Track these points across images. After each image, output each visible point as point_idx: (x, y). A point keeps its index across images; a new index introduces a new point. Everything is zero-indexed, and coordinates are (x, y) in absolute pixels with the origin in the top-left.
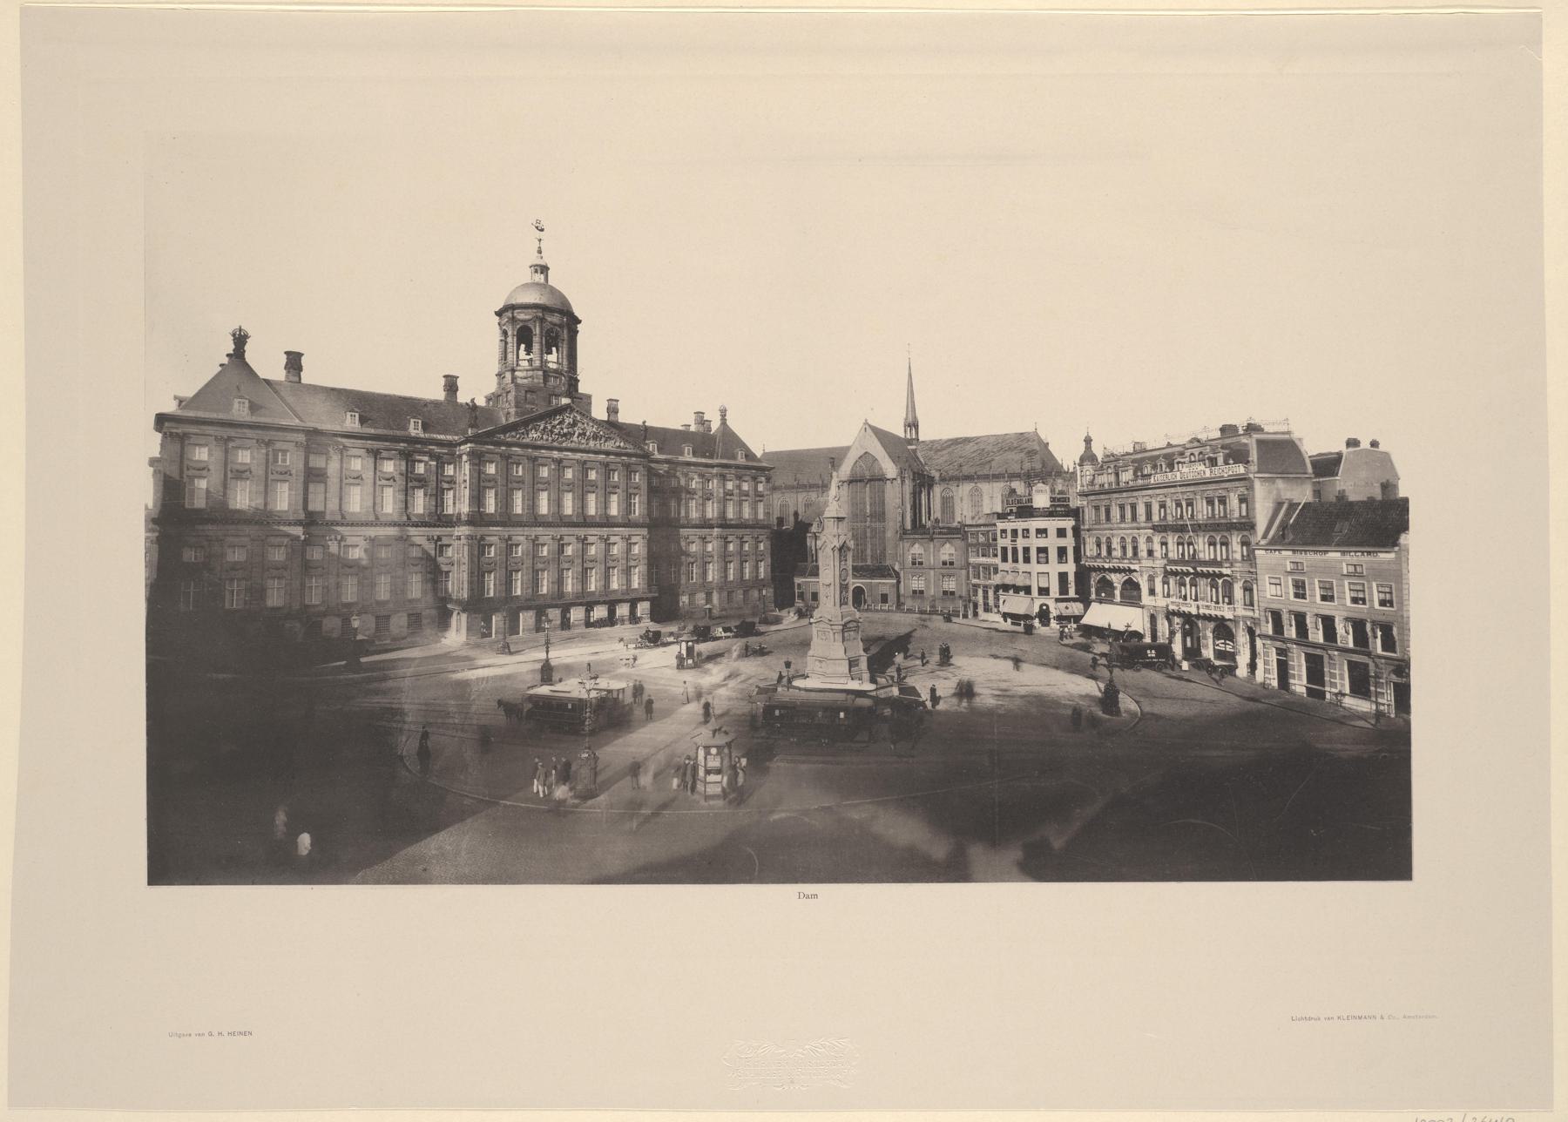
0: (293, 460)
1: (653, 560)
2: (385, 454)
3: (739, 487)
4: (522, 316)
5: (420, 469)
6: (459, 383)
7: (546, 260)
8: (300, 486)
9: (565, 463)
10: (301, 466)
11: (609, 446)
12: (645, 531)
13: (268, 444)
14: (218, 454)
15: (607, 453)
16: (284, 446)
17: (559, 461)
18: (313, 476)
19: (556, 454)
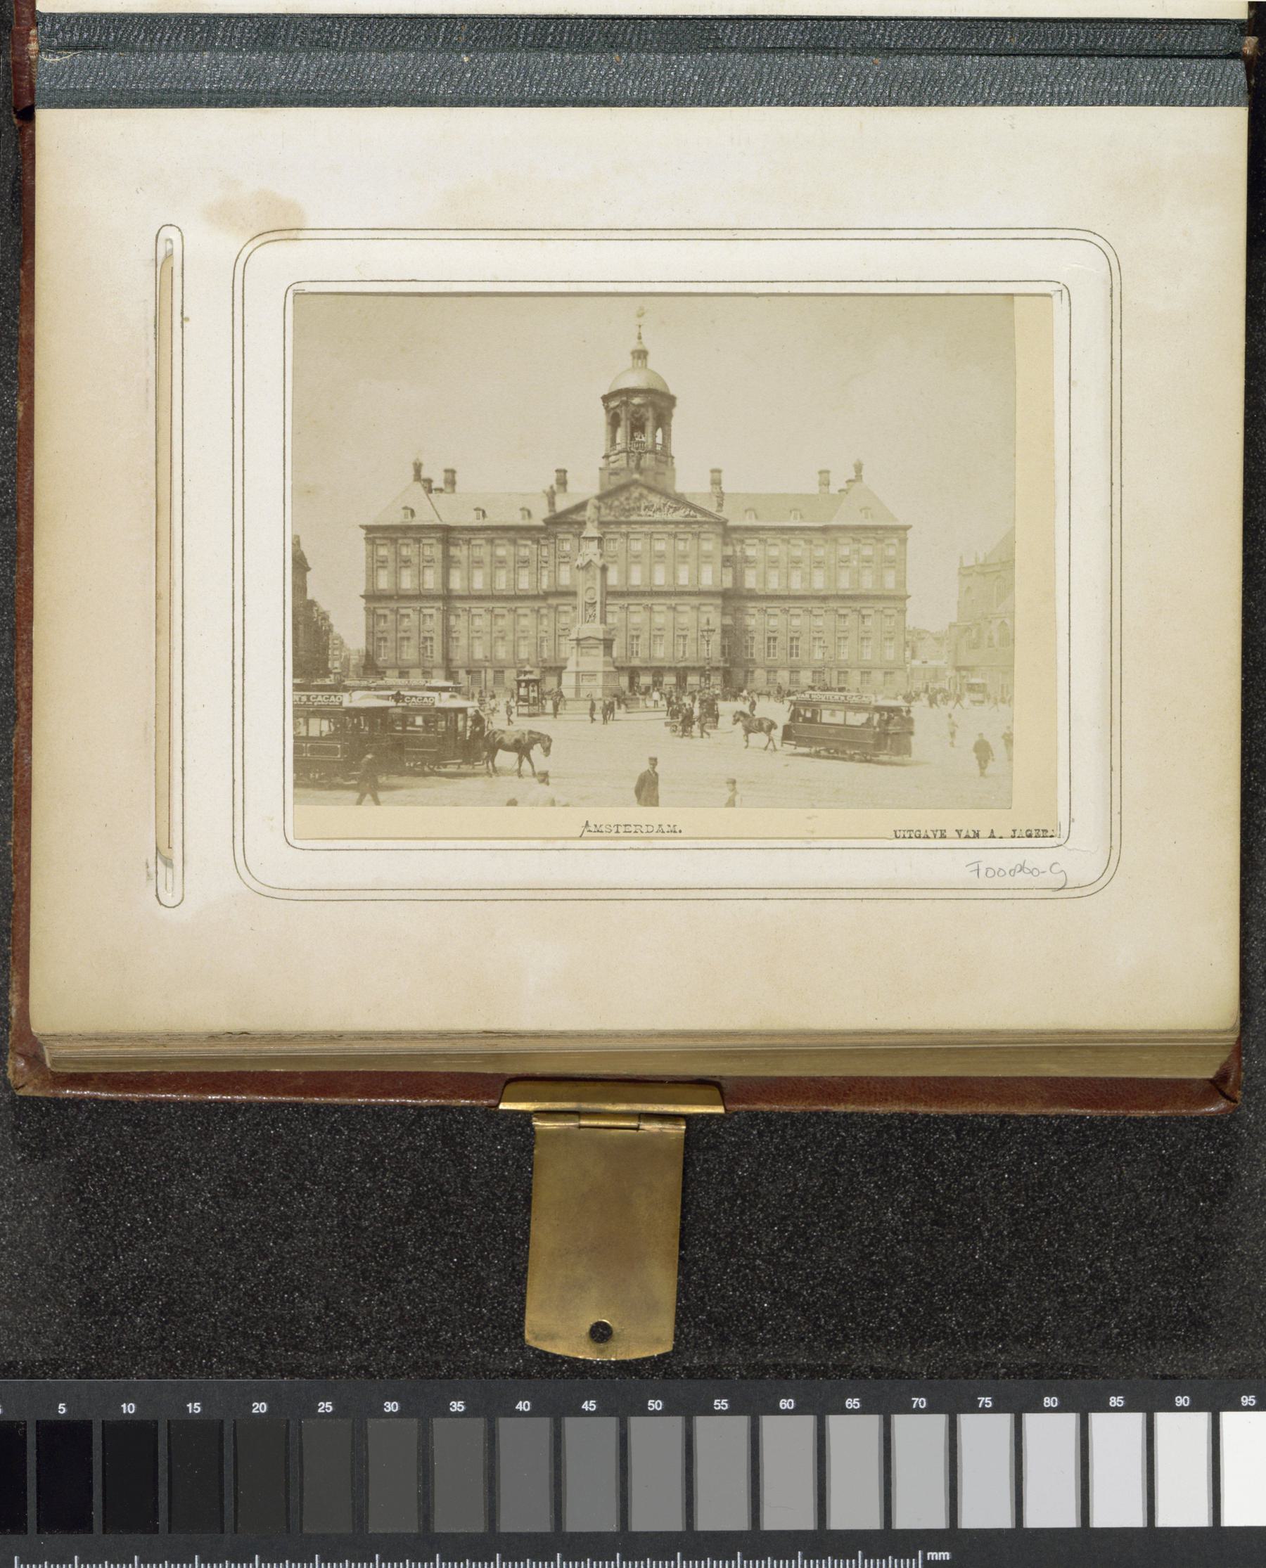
0: (436, 551)
1: (725, 631)
2: (497, 542)
3: (858, 551)
4: (613, 404)
5: (524, 552)
6: (568, 475)
7: (647, 345)
8: (440, 570)
9: (632, 536)
10: (440, 556)
11: (679, 515)
12: (719, 602)
13: (418, 541)
14: (393, 550)
15: (677, 523)
16: (430, 541)
17: (627, 535)
18: (448, 563)
19: (624, 529)
